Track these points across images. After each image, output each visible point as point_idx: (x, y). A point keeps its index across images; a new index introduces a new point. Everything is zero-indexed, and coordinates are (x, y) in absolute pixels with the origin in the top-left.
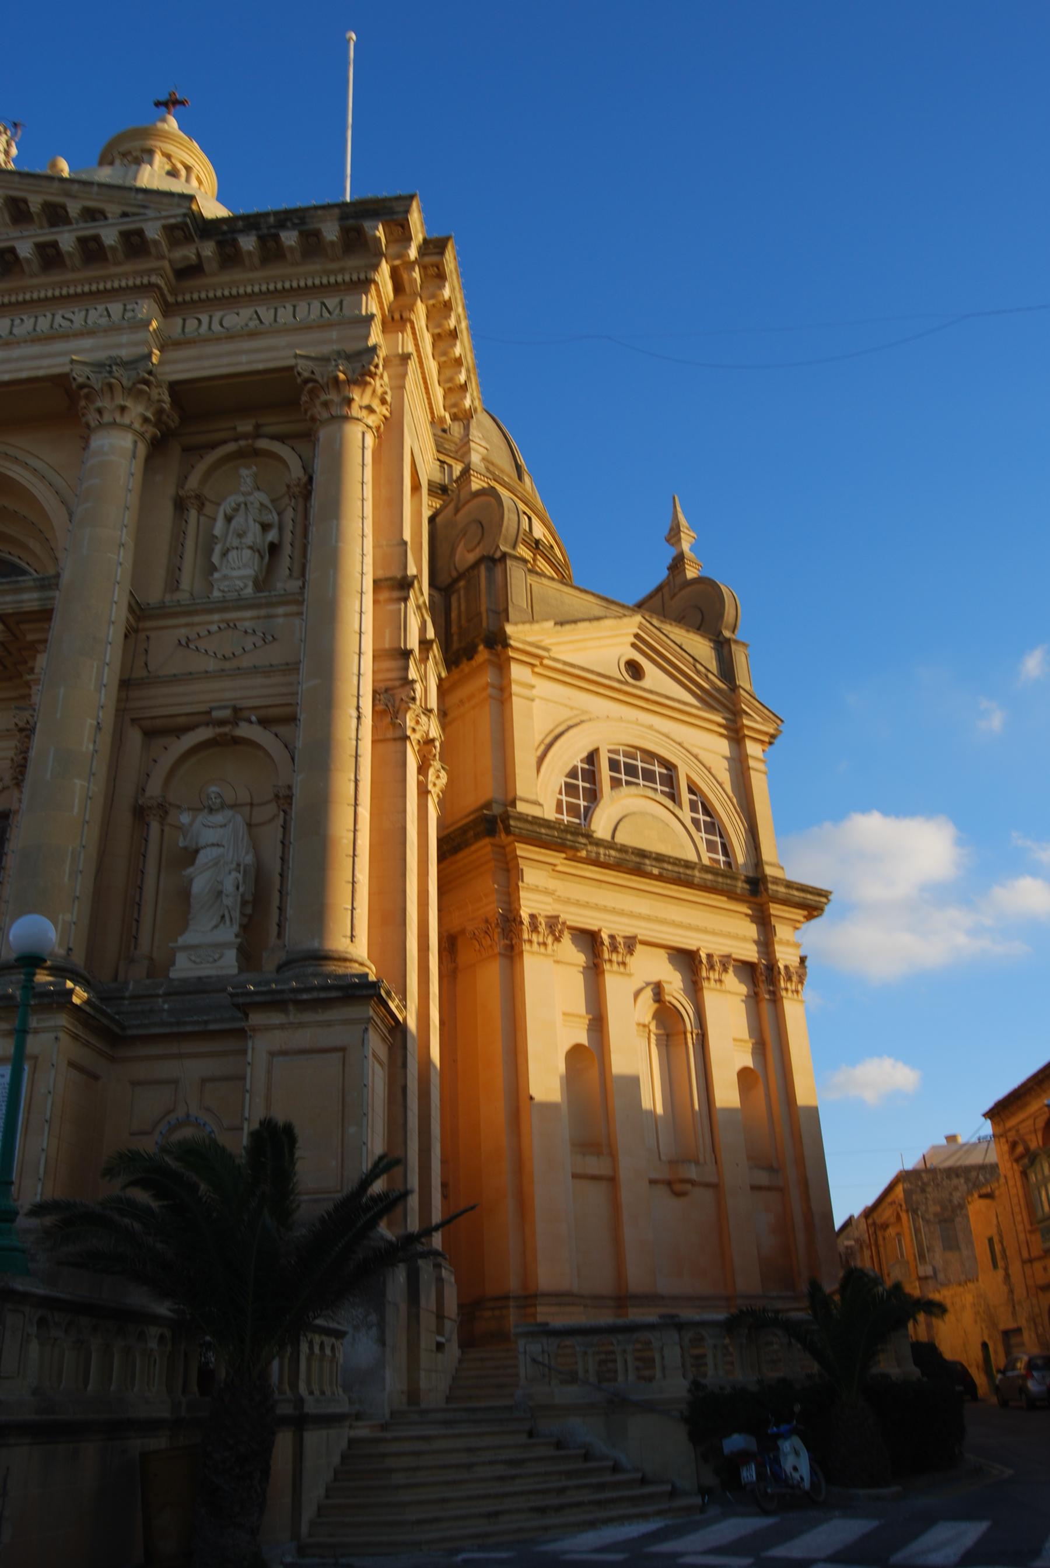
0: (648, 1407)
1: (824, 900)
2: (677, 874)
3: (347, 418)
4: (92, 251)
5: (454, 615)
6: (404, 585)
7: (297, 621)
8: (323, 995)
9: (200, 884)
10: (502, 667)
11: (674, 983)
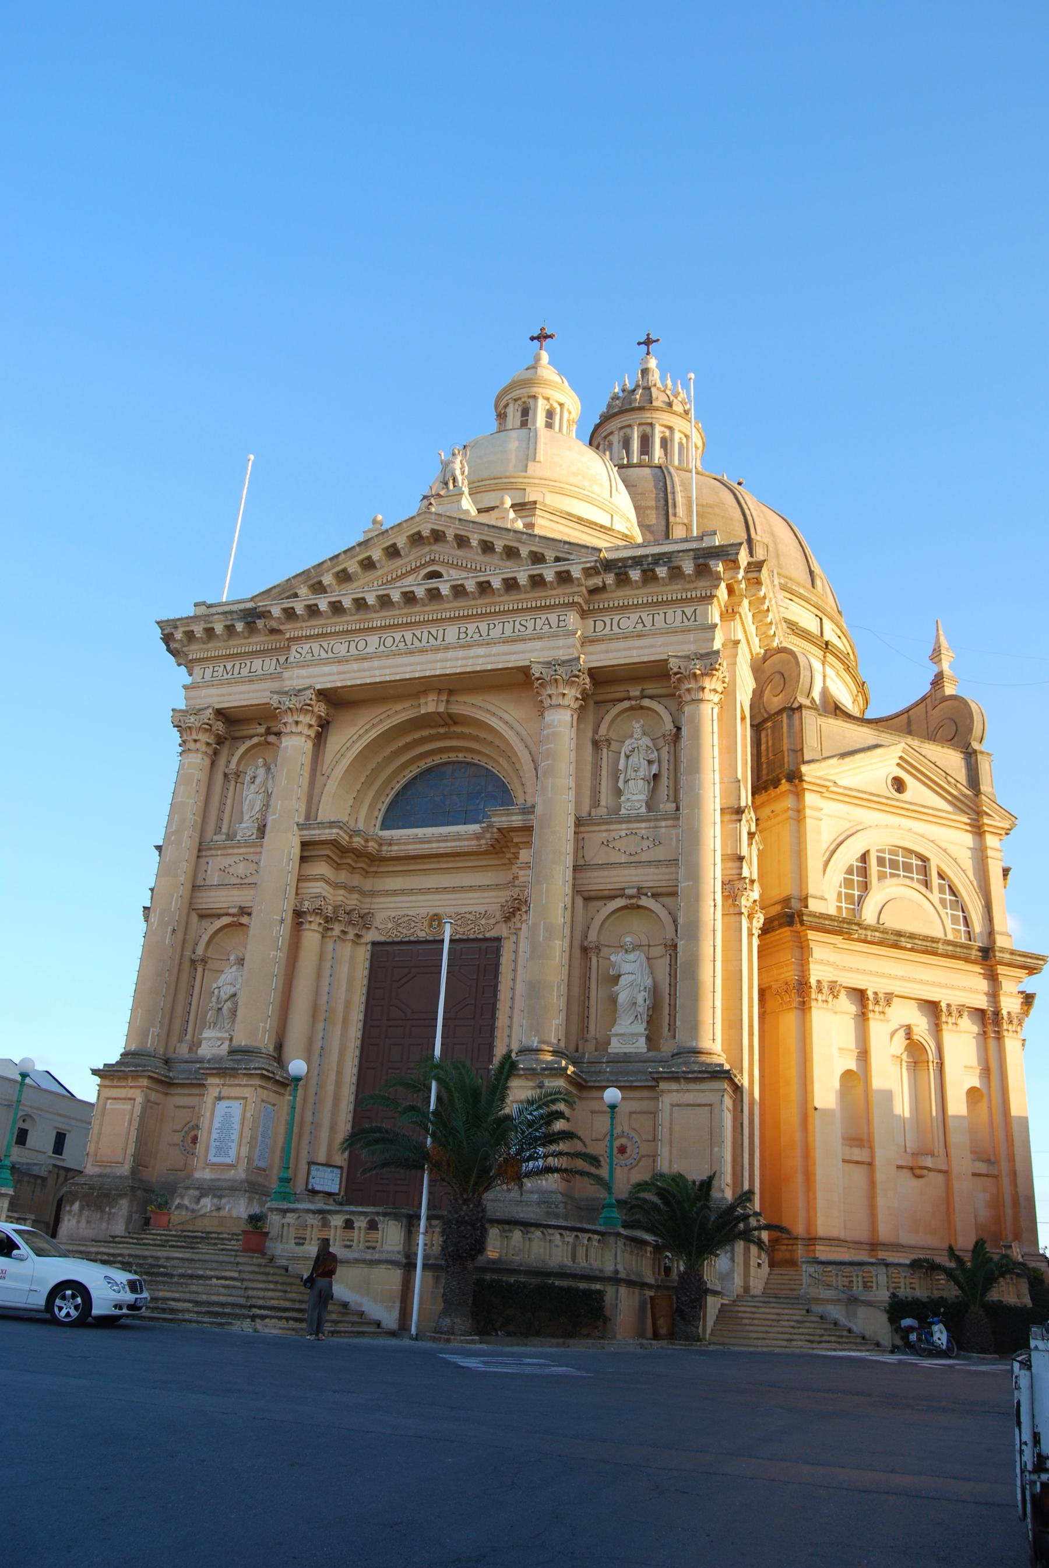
0: (869, 1304)
1: (1041, 962)
2: (927, 947)
3: (701, 700)
4: (537, 581)
5: (763, 747)
6: (739, 811)
7: (674, 831)
8: (700, 1075)
9: (622, 998)
10: (799, 794)
11: (921, 1025)
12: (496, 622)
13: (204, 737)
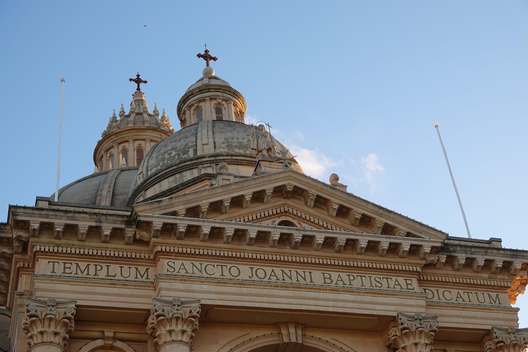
4: (394, 248)
12: (355, 275)
13: (62, 331)
